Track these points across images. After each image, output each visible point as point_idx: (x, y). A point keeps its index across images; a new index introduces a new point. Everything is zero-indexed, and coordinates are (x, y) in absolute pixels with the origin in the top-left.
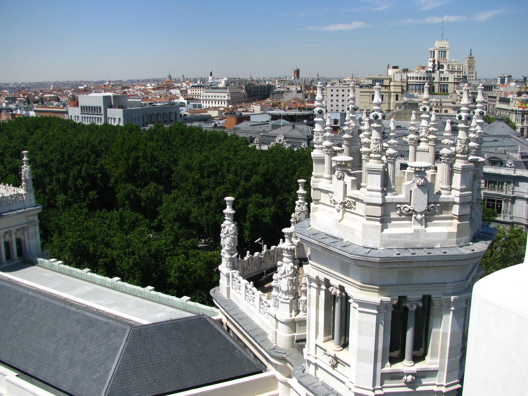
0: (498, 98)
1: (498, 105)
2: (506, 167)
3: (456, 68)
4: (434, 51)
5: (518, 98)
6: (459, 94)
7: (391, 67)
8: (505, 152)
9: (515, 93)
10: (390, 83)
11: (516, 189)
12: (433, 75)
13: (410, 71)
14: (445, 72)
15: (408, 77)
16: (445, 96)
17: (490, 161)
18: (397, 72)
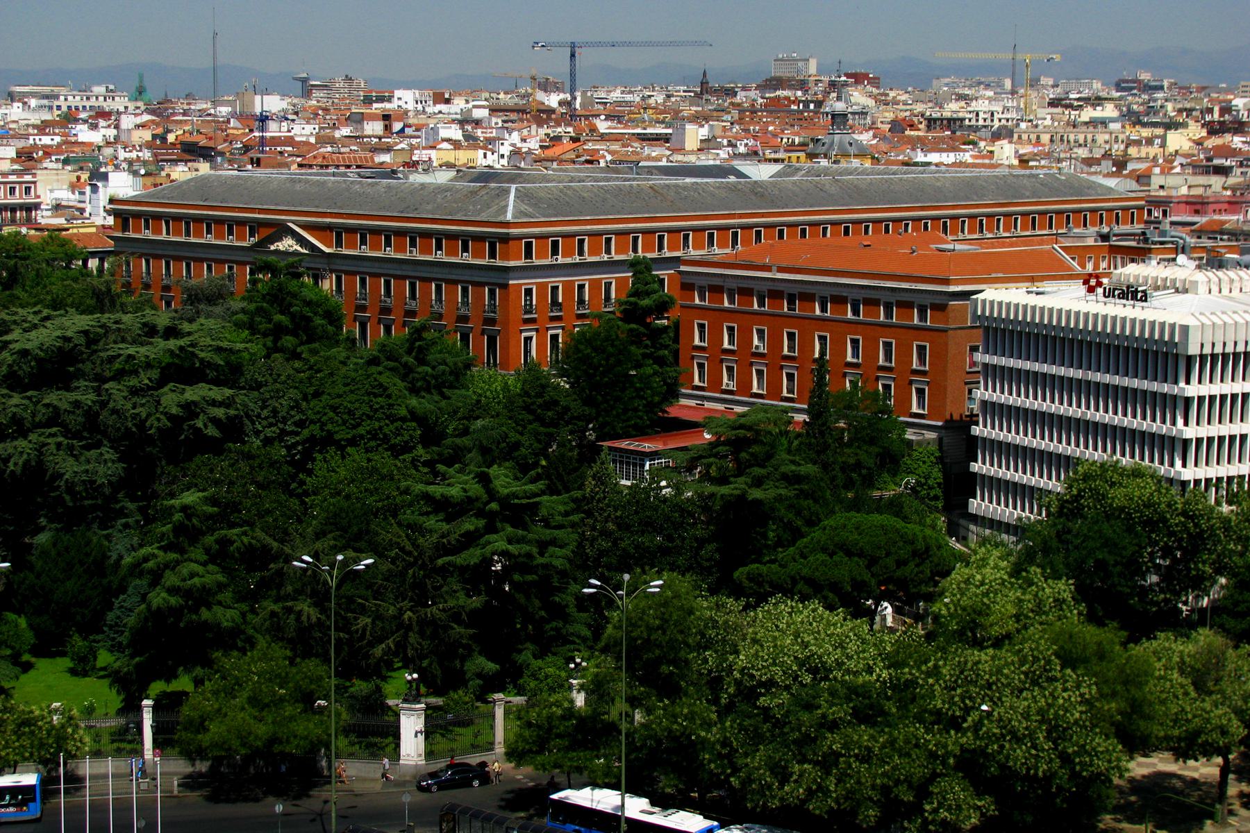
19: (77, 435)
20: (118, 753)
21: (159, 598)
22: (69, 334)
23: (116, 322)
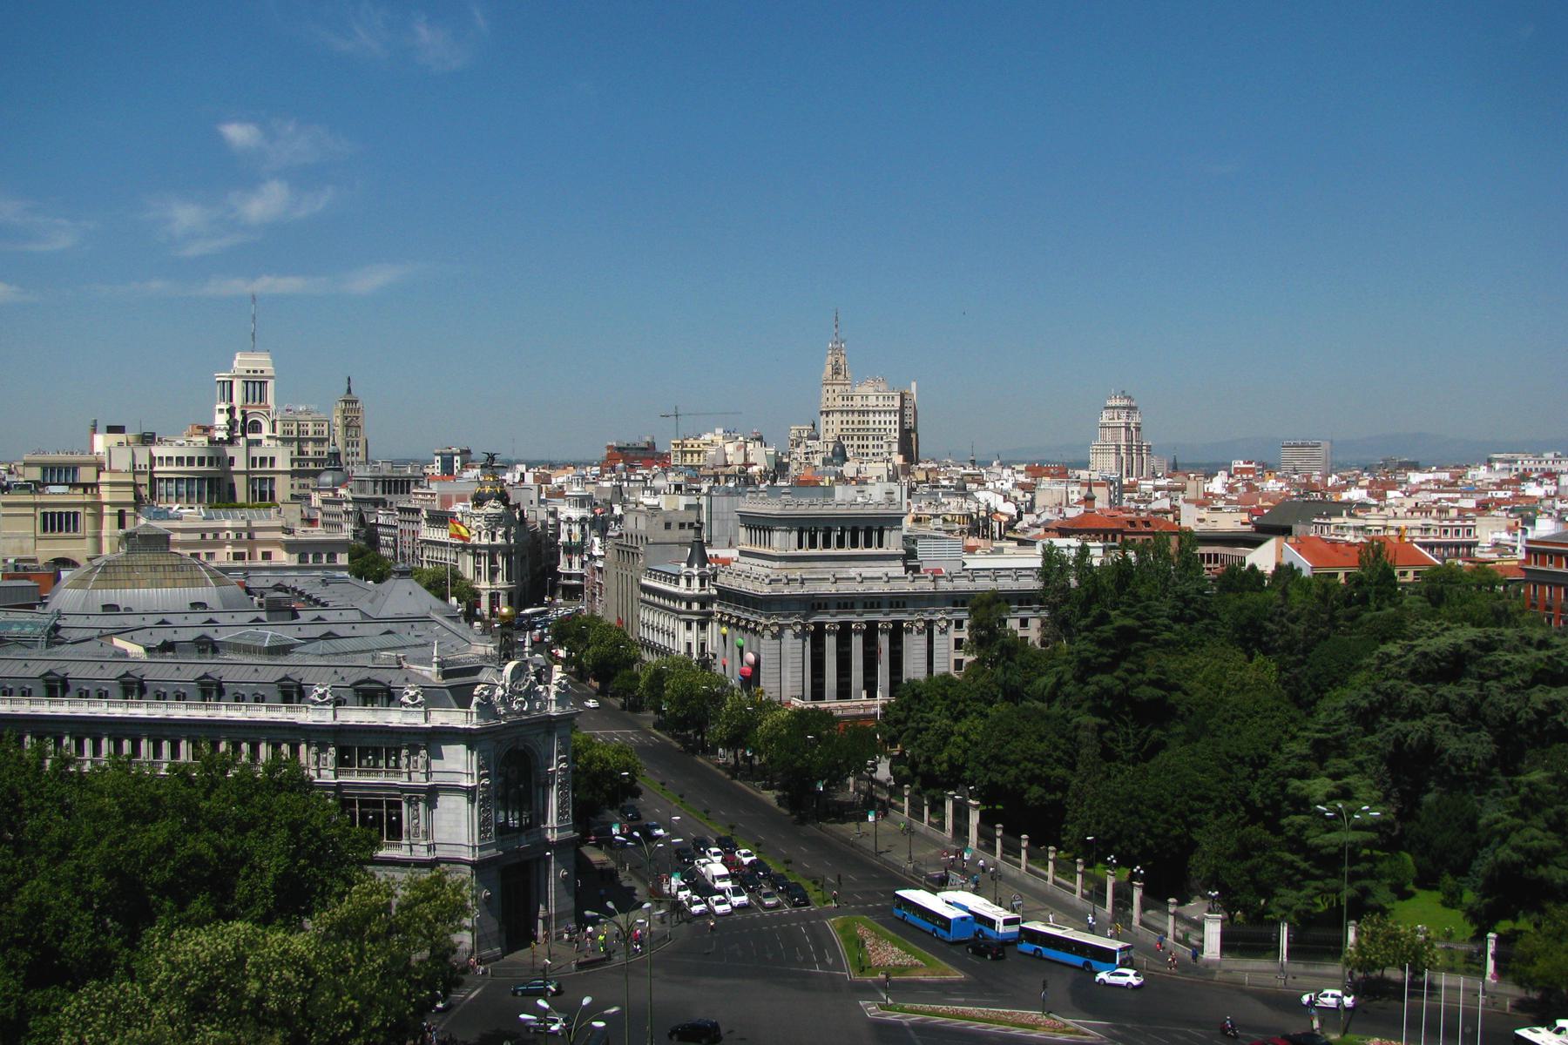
0: (425, 513)
1: (428, 533)
4: (231, 382)
6: (321, 505)
7: (102, 426)
8: (400, 663)
9: (469, 499)
10: (98, 476)
11: (436, 765)
12: (230, 451)
13: (160, 440)
14: (265, 442)
15: (152, 459)
16: (263, 512)
17: (357, 690)
18: (120, 444)
19: (1463, 721)
20: (1468, 972)
21: (1505, 853)
22: (1460, 642)
23: (1499, 635)
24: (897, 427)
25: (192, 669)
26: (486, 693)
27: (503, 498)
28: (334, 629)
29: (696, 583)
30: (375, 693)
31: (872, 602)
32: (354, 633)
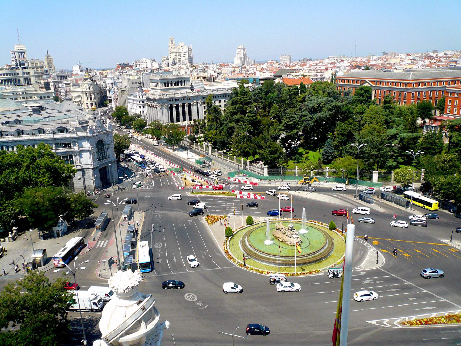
2: (70, 132)
3: (39, 64)
5: (85, 83)
12: (17, 71)
17: (58, 129)
24: (188, 56)
25: (14, 128)
26: (91, 127)
27: (91, 79)
28: (51, 115)
29: (141, 97)
30: (62, 130)
31: (183, 99)
32: (56, 115)
